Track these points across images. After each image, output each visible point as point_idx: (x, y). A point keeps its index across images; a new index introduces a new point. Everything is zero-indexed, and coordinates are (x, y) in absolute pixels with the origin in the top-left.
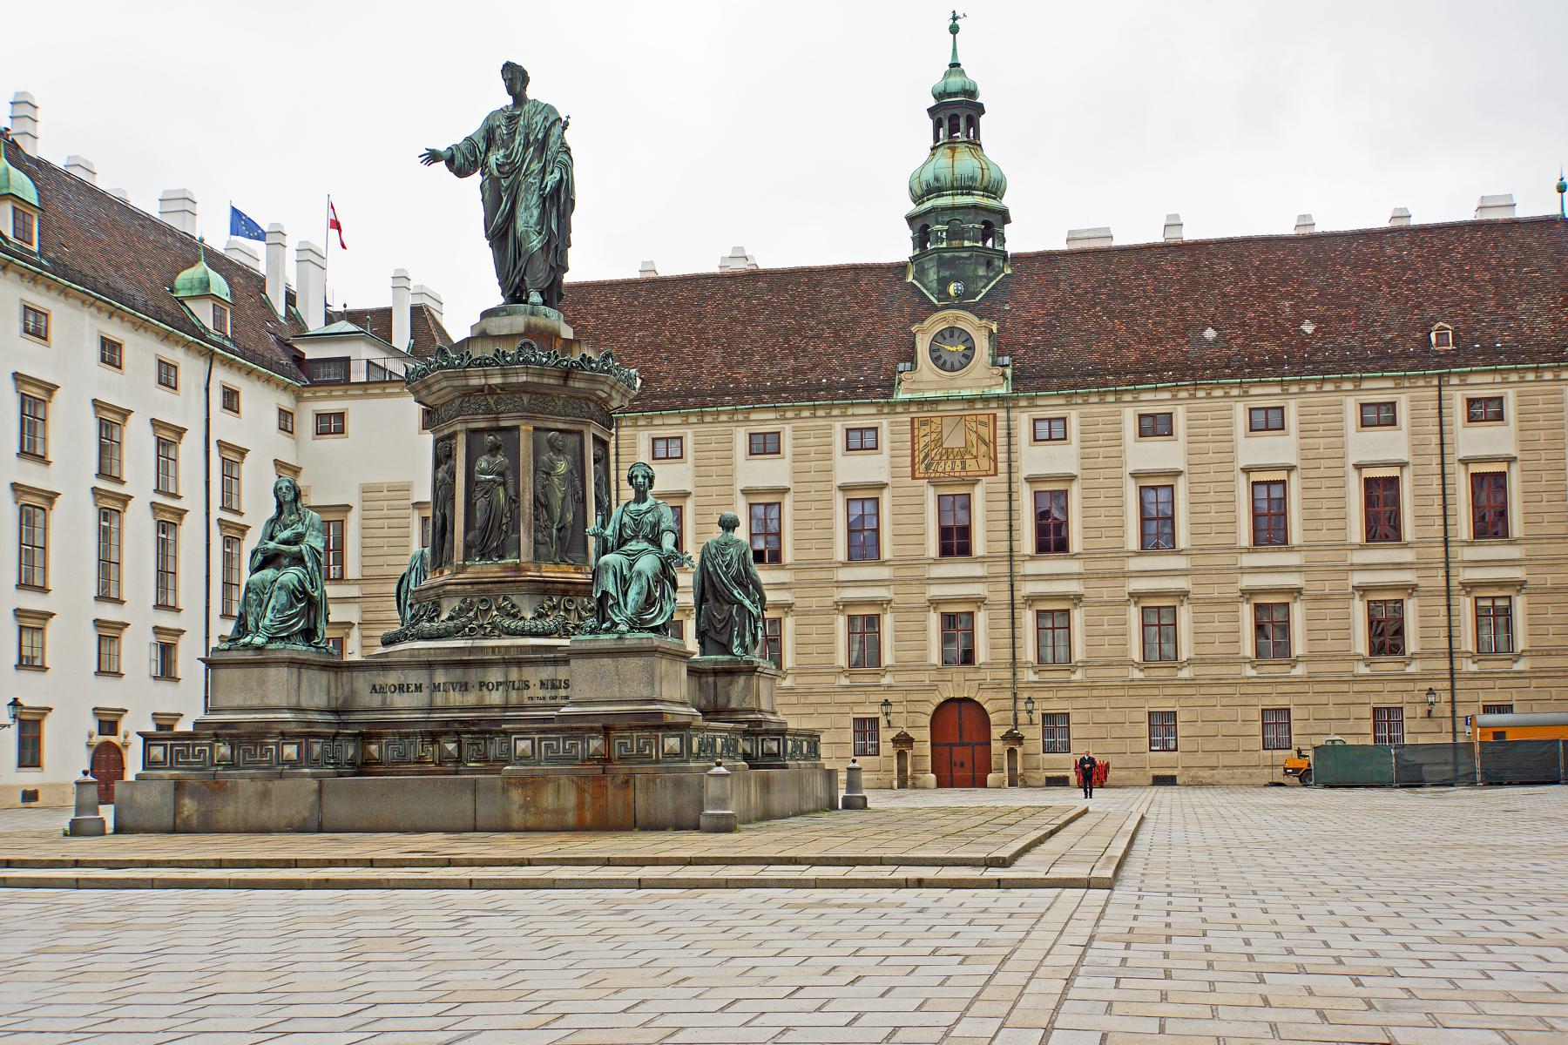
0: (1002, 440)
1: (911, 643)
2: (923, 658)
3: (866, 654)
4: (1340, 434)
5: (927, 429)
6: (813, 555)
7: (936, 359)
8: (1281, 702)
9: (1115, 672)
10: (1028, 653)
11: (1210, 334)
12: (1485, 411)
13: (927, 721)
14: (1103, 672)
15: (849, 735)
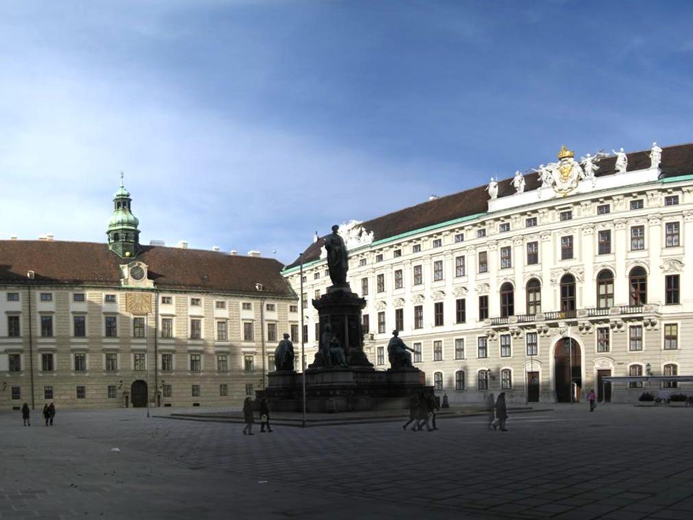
0: (153, 302)
1: (125, 363)
2: (130, 367)
3: (111, 367)
4: (238, 310)
5: (130, 297)
6: (95, 334)
7: (135, 277)
8: (225, 383)
9: (183, 373)
10: (160, 366)
11: (206, 277)
12: (270, 308)
13: (130, 387)
14: (179, 373)
15: (107, 392)
